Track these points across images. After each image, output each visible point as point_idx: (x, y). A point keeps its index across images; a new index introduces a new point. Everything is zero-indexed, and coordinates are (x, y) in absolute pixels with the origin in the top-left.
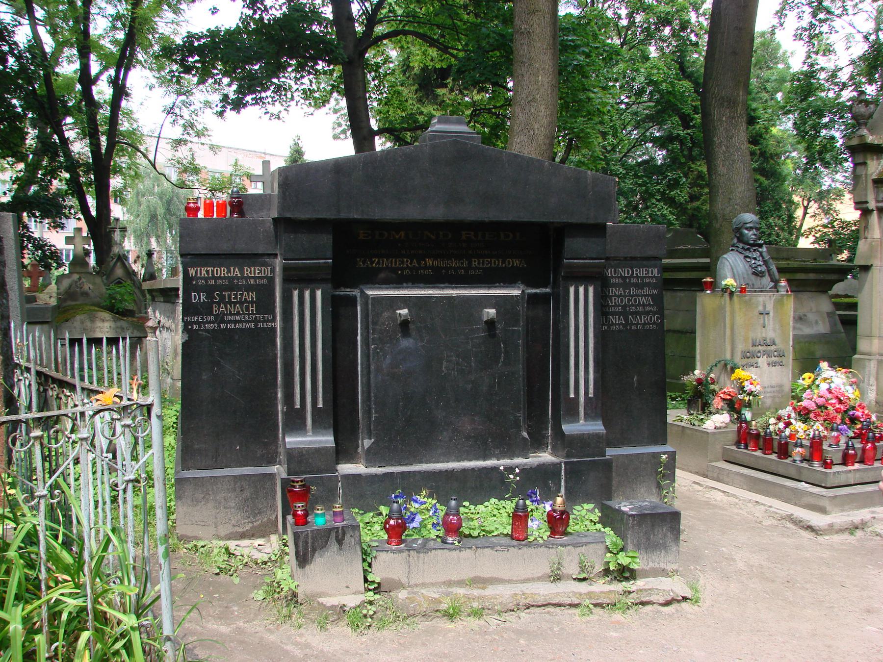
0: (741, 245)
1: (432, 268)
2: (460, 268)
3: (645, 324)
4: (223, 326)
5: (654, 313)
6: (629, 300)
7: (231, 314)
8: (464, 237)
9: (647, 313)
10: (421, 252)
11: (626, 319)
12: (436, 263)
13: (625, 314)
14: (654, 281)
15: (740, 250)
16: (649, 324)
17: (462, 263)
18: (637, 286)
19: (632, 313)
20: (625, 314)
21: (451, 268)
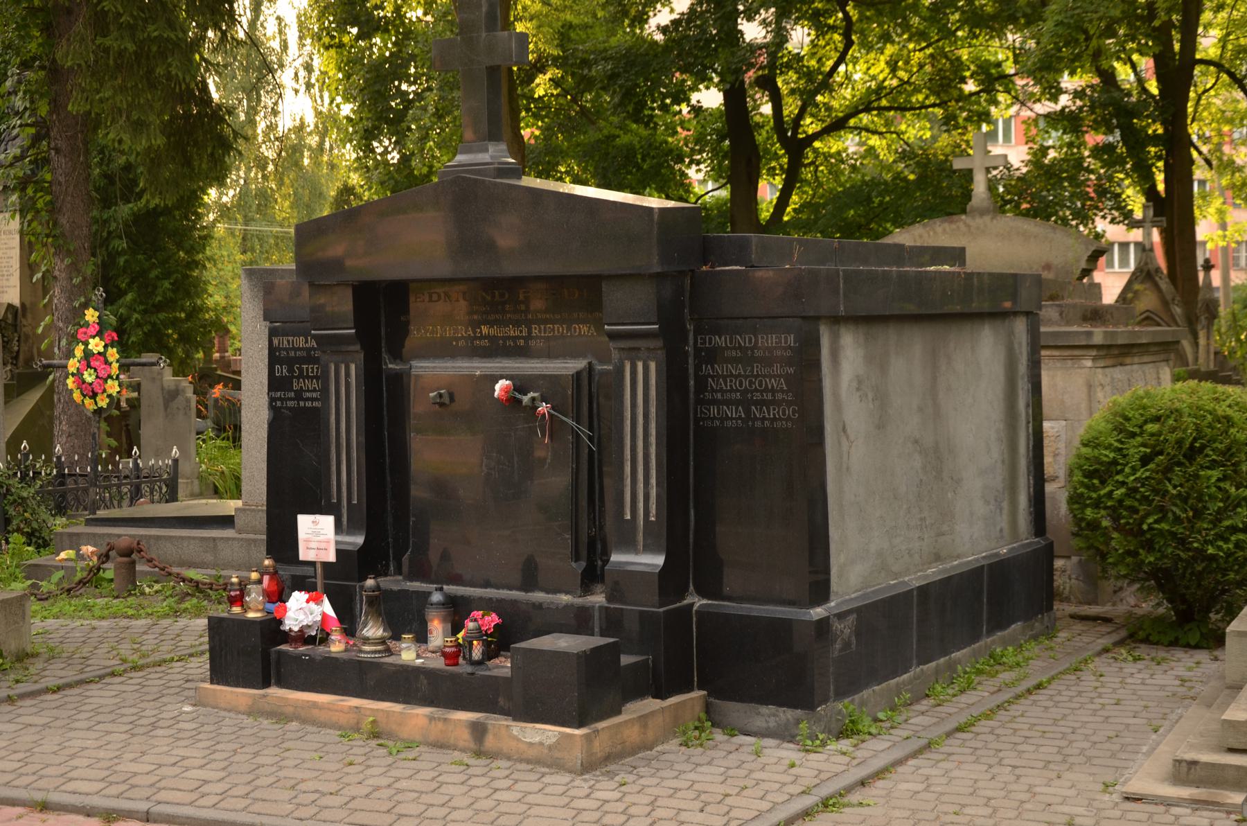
6: (751, 382)
8: (521, 297)
11: (748, 411)
12: (493, 331)
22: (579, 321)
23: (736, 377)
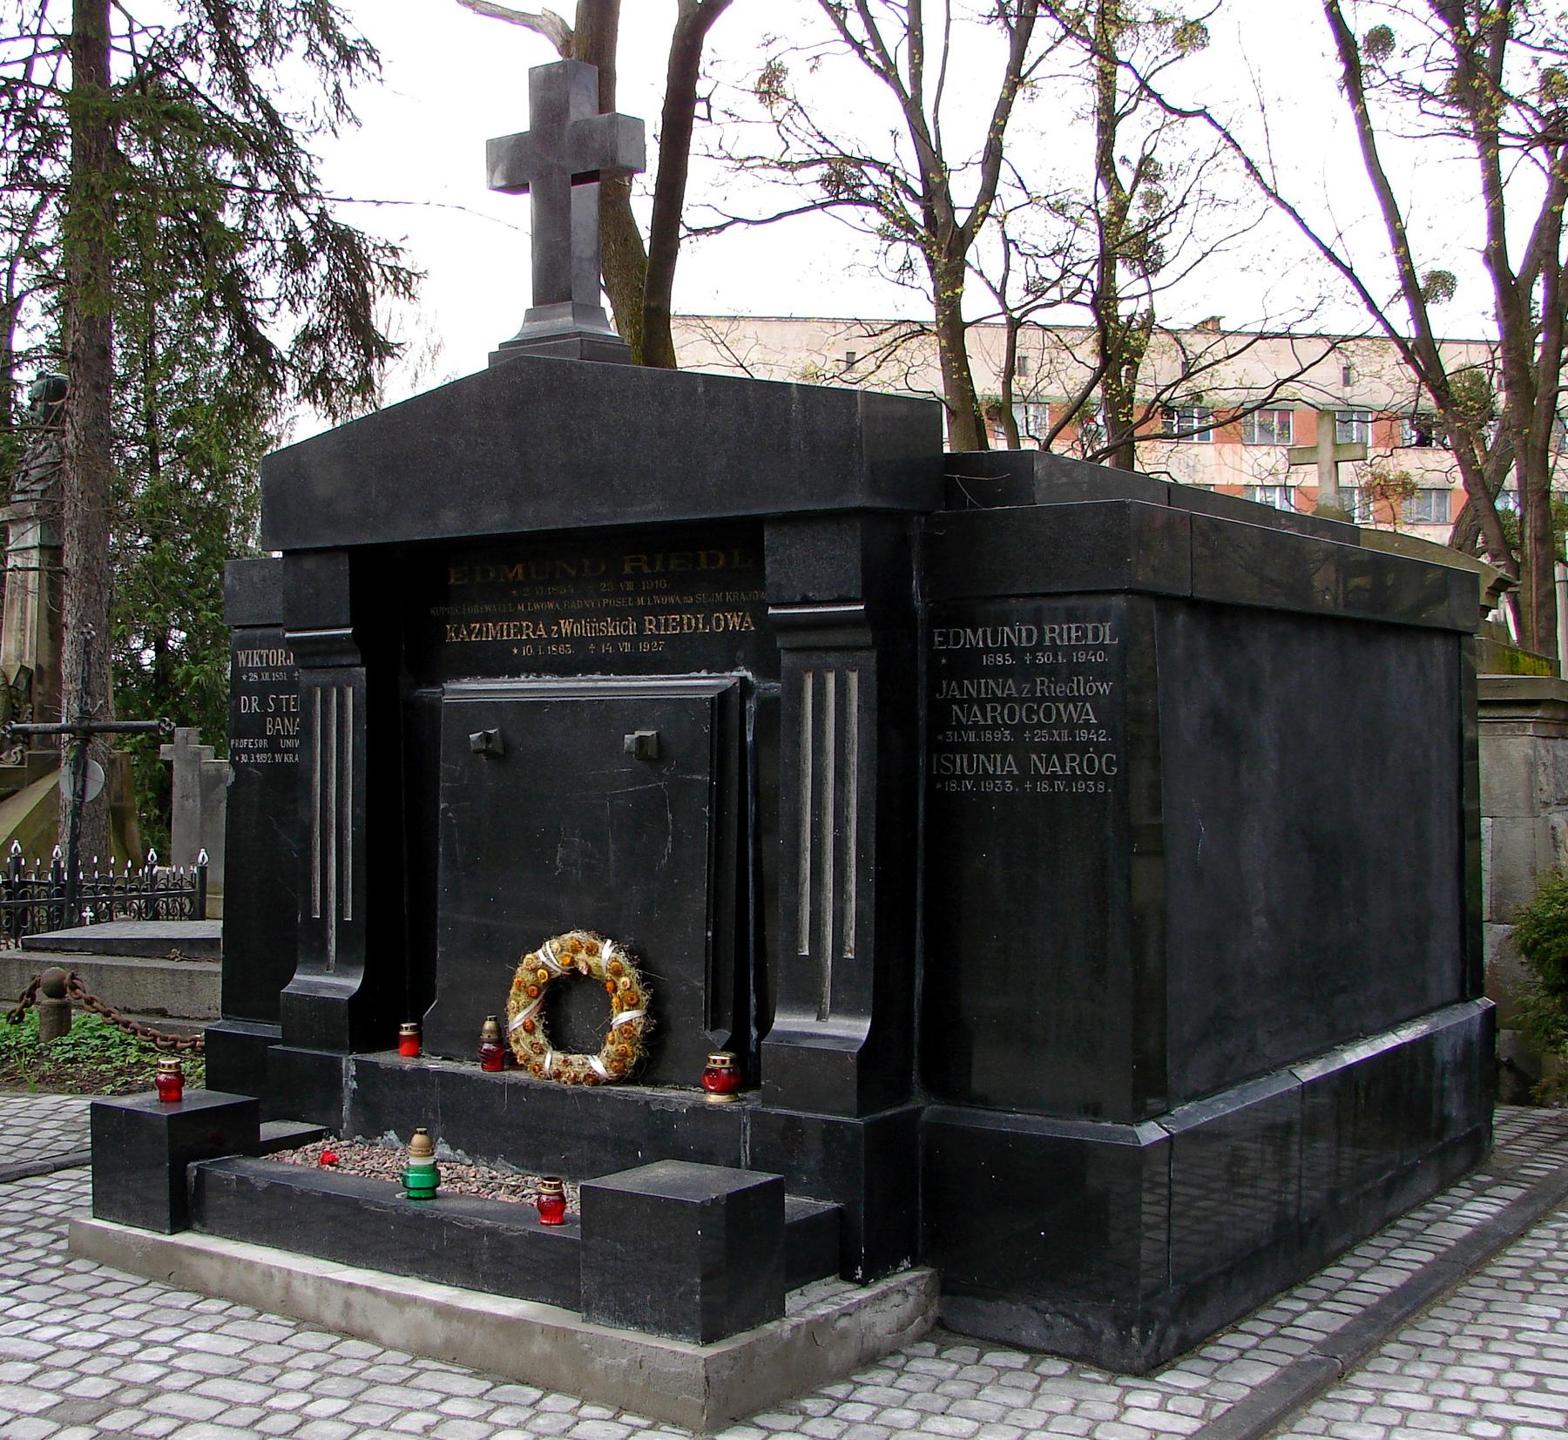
2: (621, 638)
6: (1030, 711)
8: (627, 570)
9: (1082, 748)
11: (1023, 763)
12: (578, 630)
17: (626, 628)
22: (726, 607)
23: (1003, 701)
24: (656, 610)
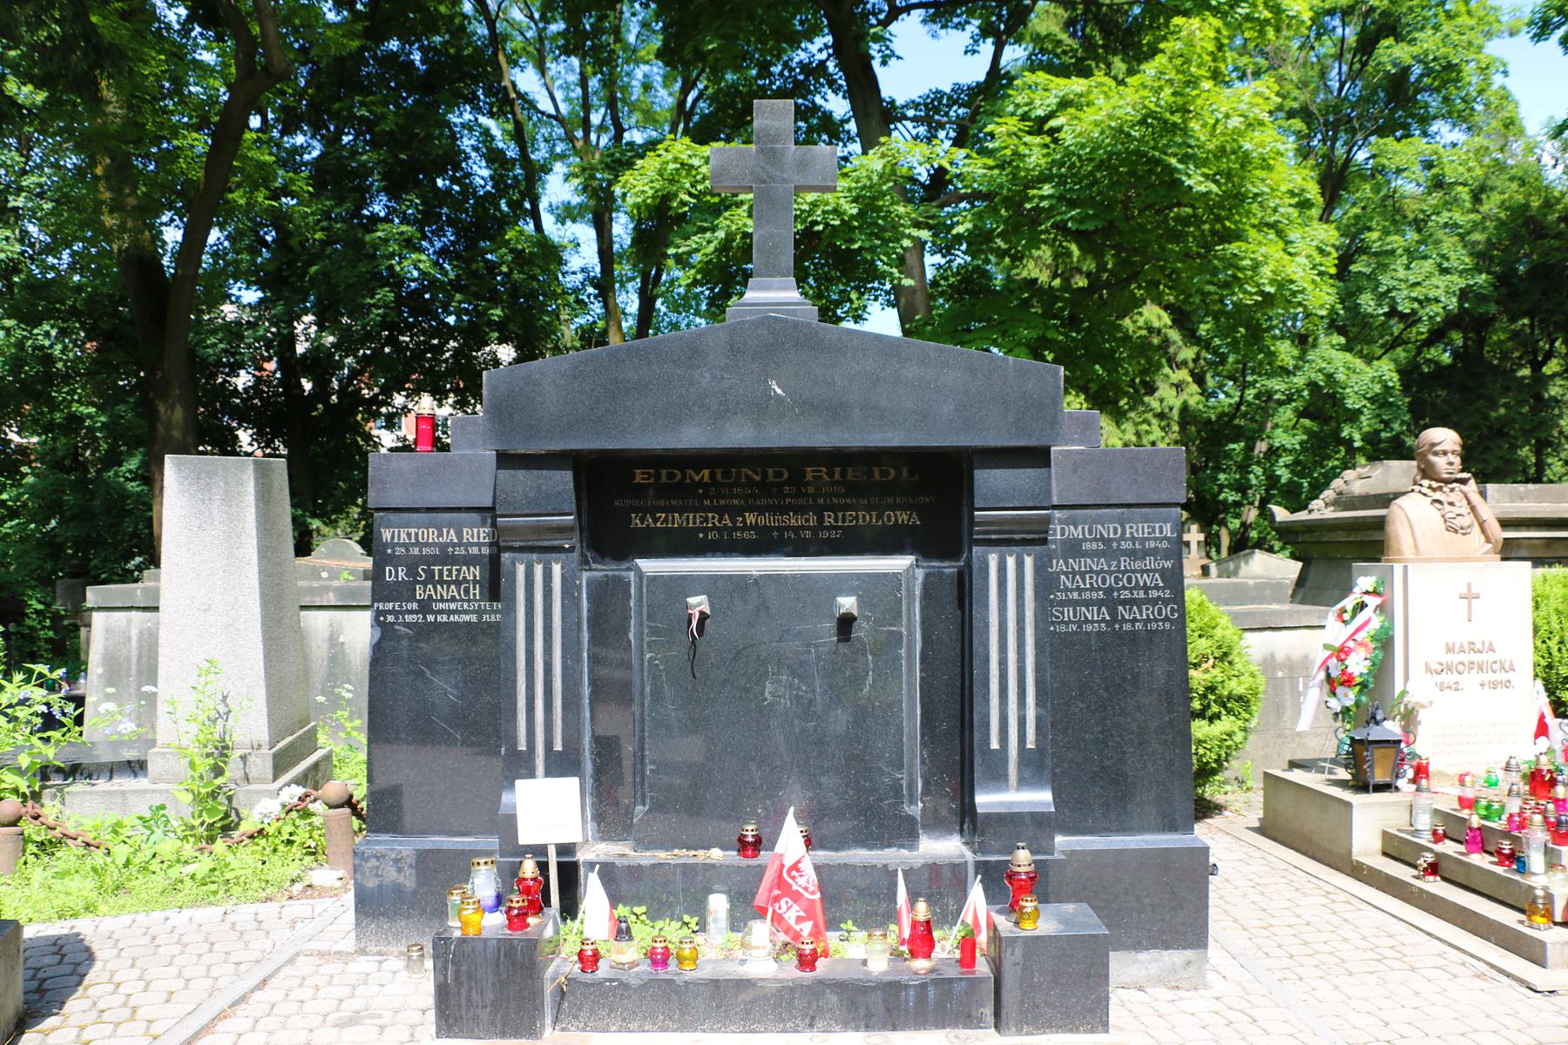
0: (1426, 483)
1: (755, 527)
2: (803, 528)
3: (1148, 620)
4: (430, 618)
5: (1166, 602)
7: (442, 600)
8: (809, 477)
9: (1154, 602)
10: (736, 502)
11: (1113, 613)
12: (762, 521)
13: (1110, 602)
14: (1165, 545)
15: (1424, 490)
16: (1156, 620)
17: (807, 520)
18: (1132, 554)
19: (1124, 602)
20: (1110, 602)
21: (788, 528)
23: (1097, 573)
24: (834, 509)
